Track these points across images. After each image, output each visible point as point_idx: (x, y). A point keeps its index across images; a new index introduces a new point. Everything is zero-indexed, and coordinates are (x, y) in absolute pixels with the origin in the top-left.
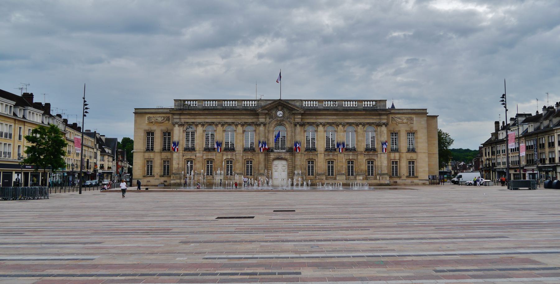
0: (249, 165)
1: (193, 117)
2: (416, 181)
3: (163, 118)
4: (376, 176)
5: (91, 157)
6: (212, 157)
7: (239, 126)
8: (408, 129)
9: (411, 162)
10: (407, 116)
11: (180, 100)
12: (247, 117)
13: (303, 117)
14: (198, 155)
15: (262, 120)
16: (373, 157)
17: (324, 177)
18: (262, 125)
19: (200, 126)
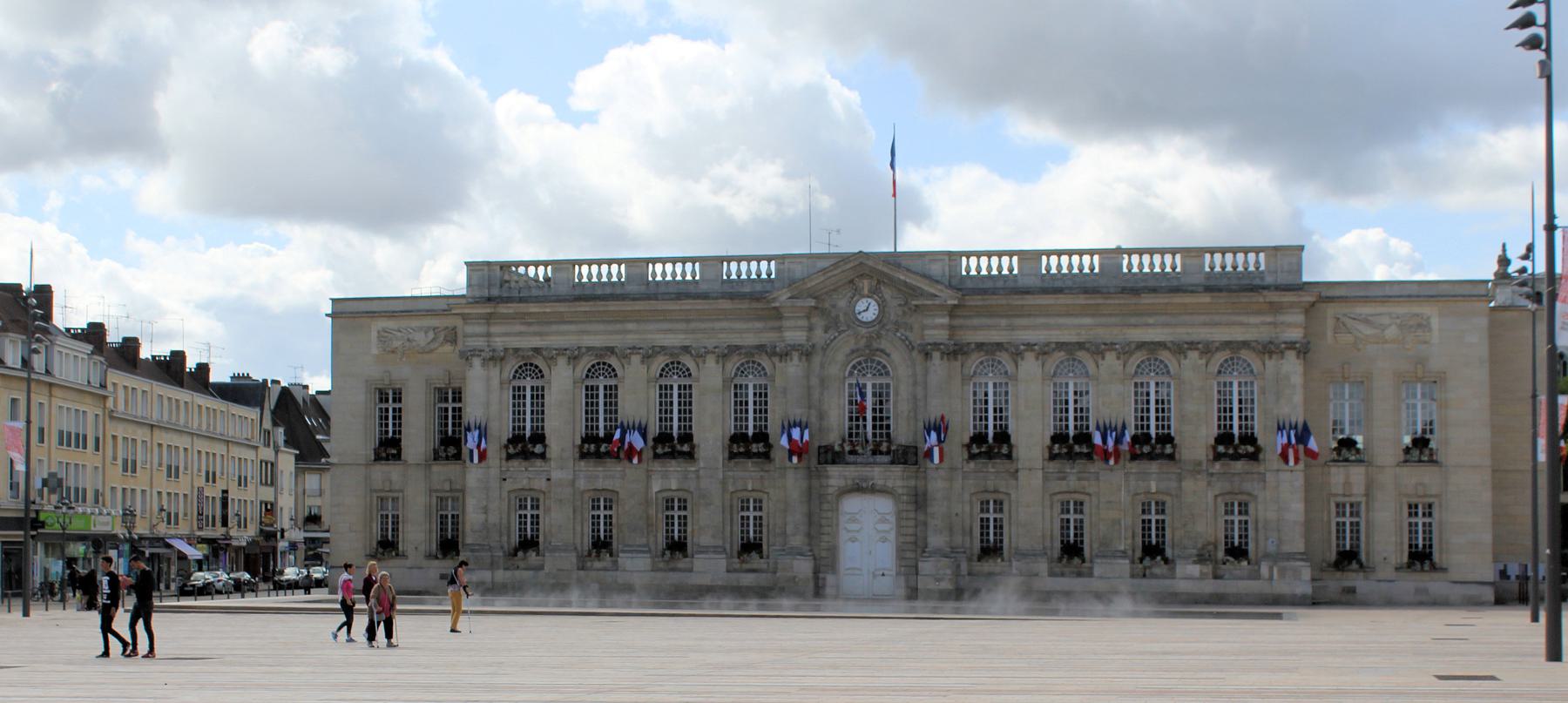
0: (751, 514)
1: (535, 328)
2: (1436, 585)
3: (431, 335)
4: (1258, 563)
5: (242, 482)
6: (608, 484)
7: (711, 362)
10: (1401, 310)
11: (489, 264)
13: (957, 322)
14: (556, 475)
15: (794, 335)
16: (1247, 486)
18: (795, 355)
19: (562, 361)
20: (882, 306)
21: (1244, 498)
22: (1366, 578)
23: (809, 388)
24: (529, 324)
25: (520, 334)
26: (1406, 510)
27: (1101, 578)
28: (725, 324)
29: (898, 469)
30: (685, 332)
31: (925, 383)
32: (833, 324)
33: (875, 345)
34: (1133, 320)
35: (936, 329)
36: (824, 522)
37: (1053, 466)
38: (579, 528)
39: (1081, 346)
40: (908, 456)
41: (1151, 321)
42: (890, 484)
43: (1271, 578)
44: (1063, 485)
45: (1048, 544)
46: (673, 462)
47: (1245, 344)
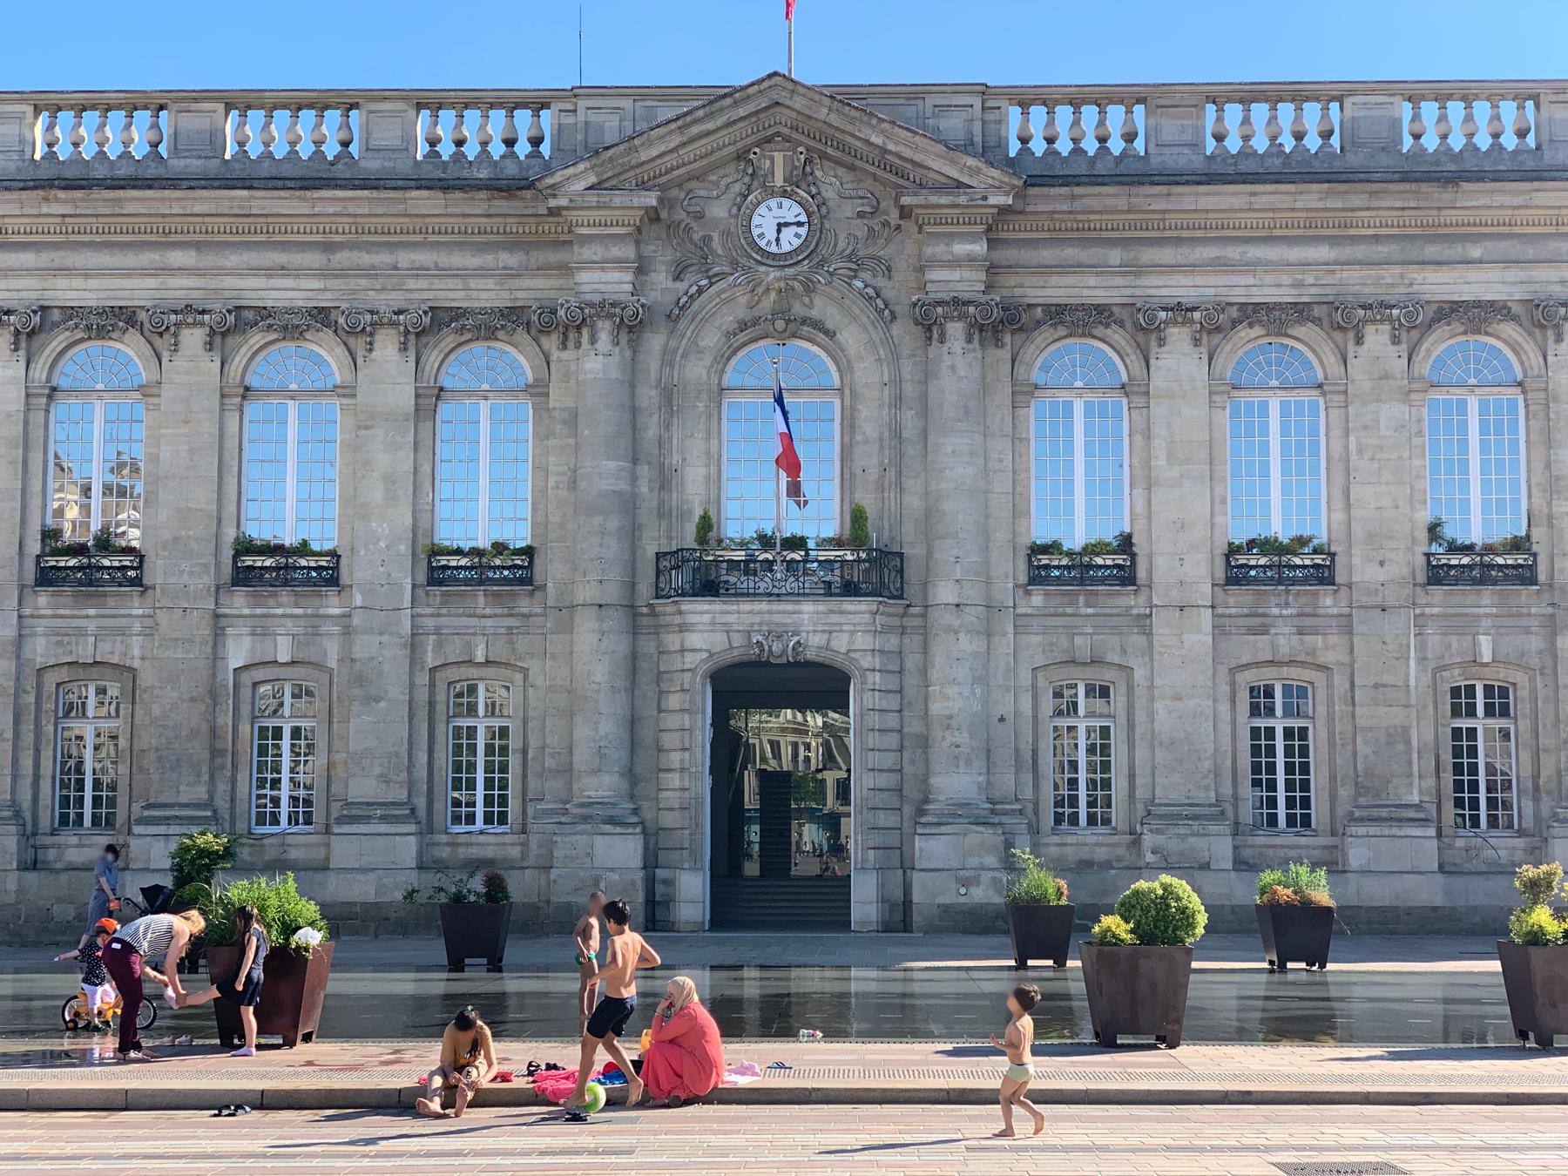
7: (387, 347)
13: (1005, 255)
15: (603, 279)
18: (605, 329)
20: (818, 214)
23: (634, 411)
28: (423, 257)
29: (859, 608)
30: (322, 273)
31: (924, 397)
32: (696, 261)
33: (798, 309)
34: (1431, 251)
35: (956, 266)
36: (669, 740)
37: (1239, 599)
38: (27, 763)
39: (1301, 312)
41: (1476, 252)
42: (841, 643)
44: (1261, 647)
45: (1227, 791)
46: (285, 595)
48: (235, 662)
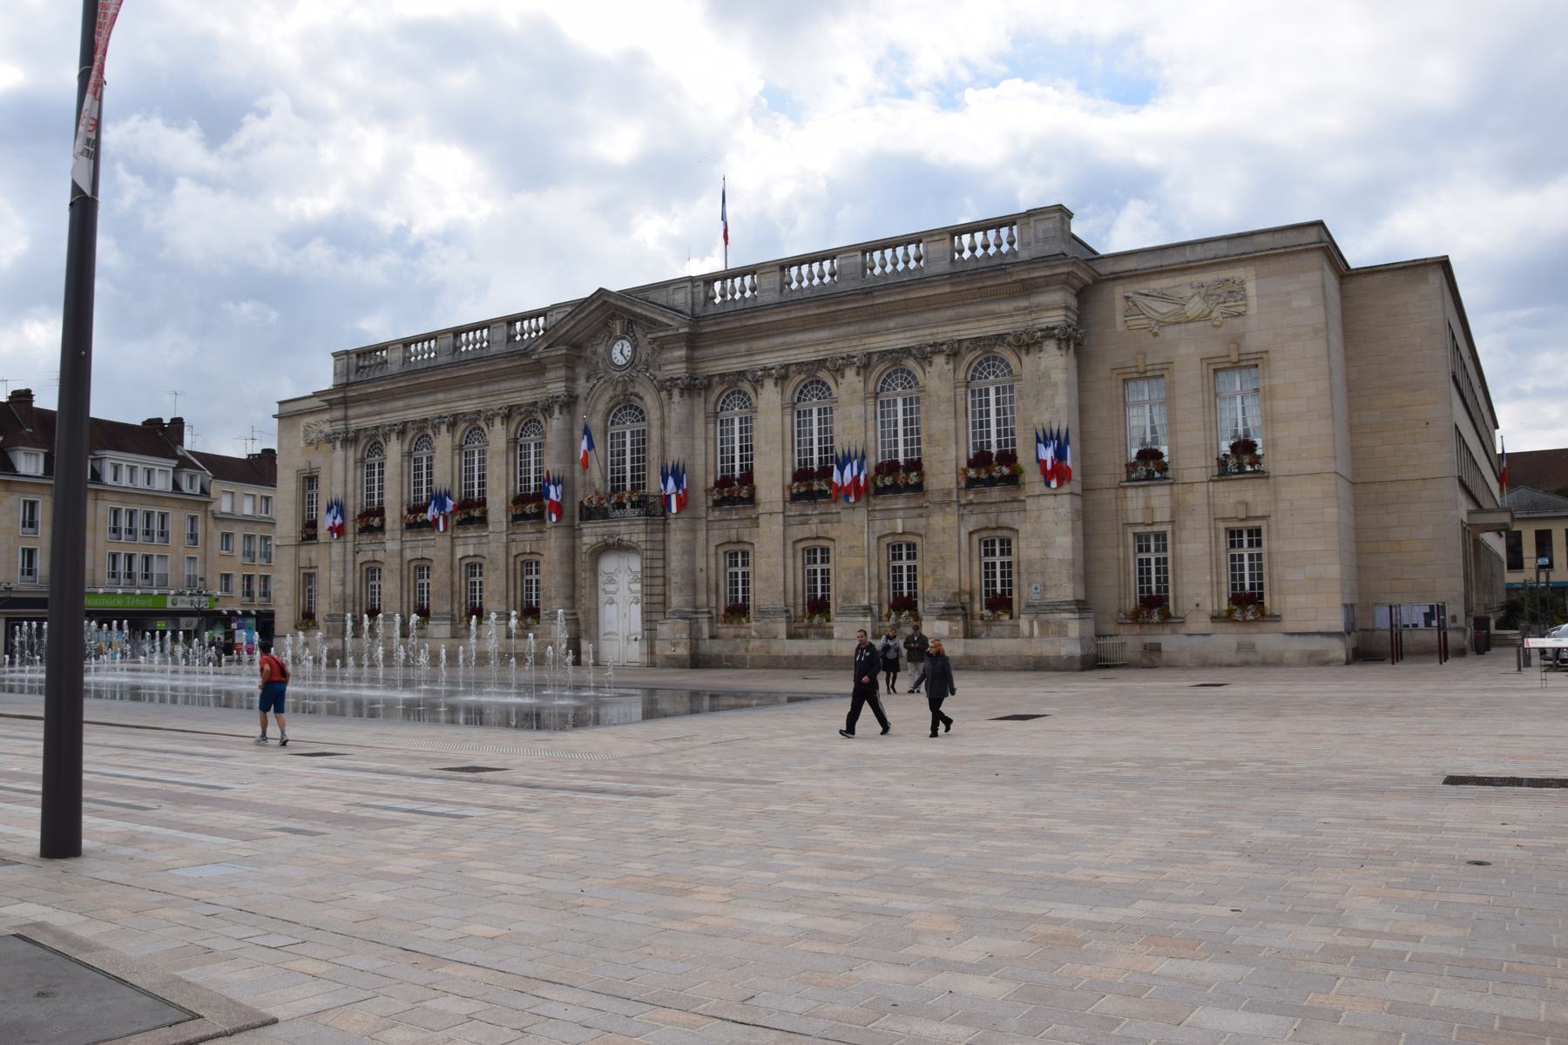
1: (376, 408)
2: (1266, 640)
8: (1215, 349)
9: (1245, 535)
10: (1208, 277)
12: (518, 384)
13: (698, 354)
16: (1006, 519)
17: (781, 628)
20: (635, 348)
21: (1005, 534)
22: (1174, 632)
24: (373, 404)
25: (367, 415)
26: (1223, 539)
27: (840, 639)
33: (631, 390)
34: (873, 326)
37: (794, 510)
40: (653, 510)
41: (892, 324)
42: (635, 538)
43: (1031, 636)
45: (790, 600)
47: (1000, 338)
48: (459, 556)
